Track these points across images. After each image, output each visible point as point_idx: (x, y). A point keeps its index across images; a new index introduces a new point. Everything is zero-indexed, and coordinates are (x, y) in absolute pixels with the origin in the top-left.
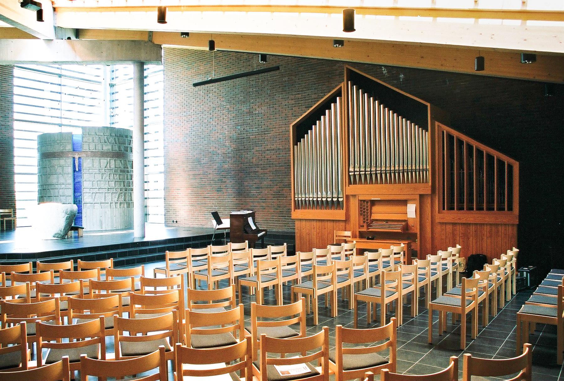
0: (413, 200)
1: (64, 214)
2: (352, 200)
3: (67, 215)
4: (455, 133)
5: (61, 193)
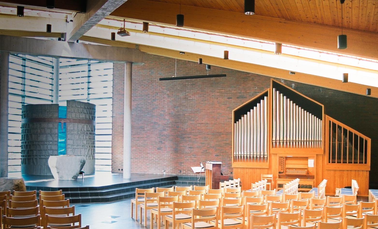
0: (312, 157)
3: (81, 164)
4: (337, 123)
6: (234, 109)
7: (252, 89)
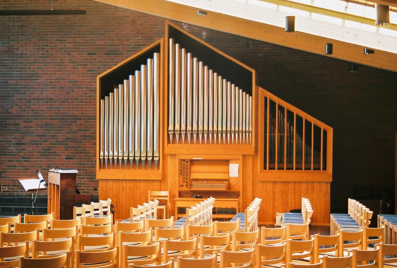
0: (236, 160)
2: (169, 160)
4: (278, 100)
6: (100, 74)
7: (132, 38)
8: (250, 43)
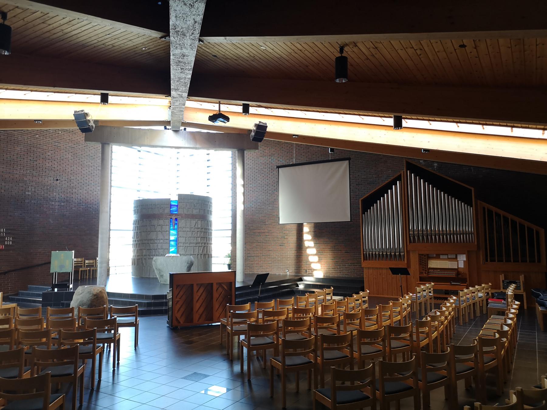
1: (186, 264)
5: (159, 247)
6: (361, 197)
8: (472, 168)
